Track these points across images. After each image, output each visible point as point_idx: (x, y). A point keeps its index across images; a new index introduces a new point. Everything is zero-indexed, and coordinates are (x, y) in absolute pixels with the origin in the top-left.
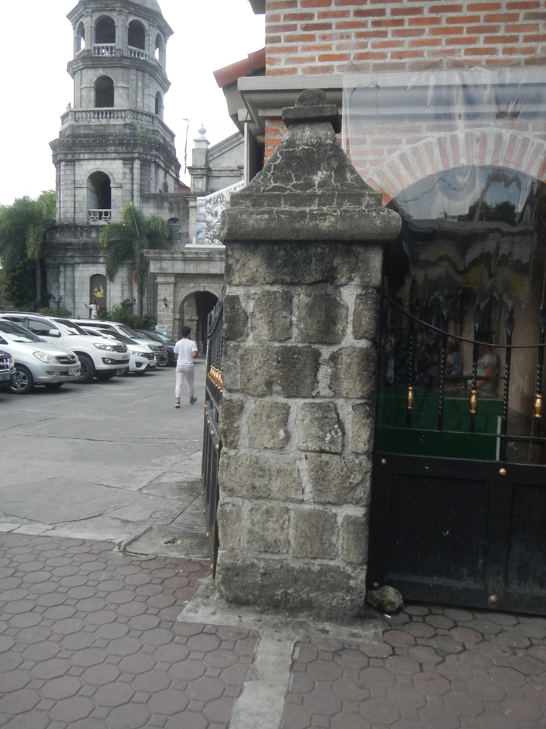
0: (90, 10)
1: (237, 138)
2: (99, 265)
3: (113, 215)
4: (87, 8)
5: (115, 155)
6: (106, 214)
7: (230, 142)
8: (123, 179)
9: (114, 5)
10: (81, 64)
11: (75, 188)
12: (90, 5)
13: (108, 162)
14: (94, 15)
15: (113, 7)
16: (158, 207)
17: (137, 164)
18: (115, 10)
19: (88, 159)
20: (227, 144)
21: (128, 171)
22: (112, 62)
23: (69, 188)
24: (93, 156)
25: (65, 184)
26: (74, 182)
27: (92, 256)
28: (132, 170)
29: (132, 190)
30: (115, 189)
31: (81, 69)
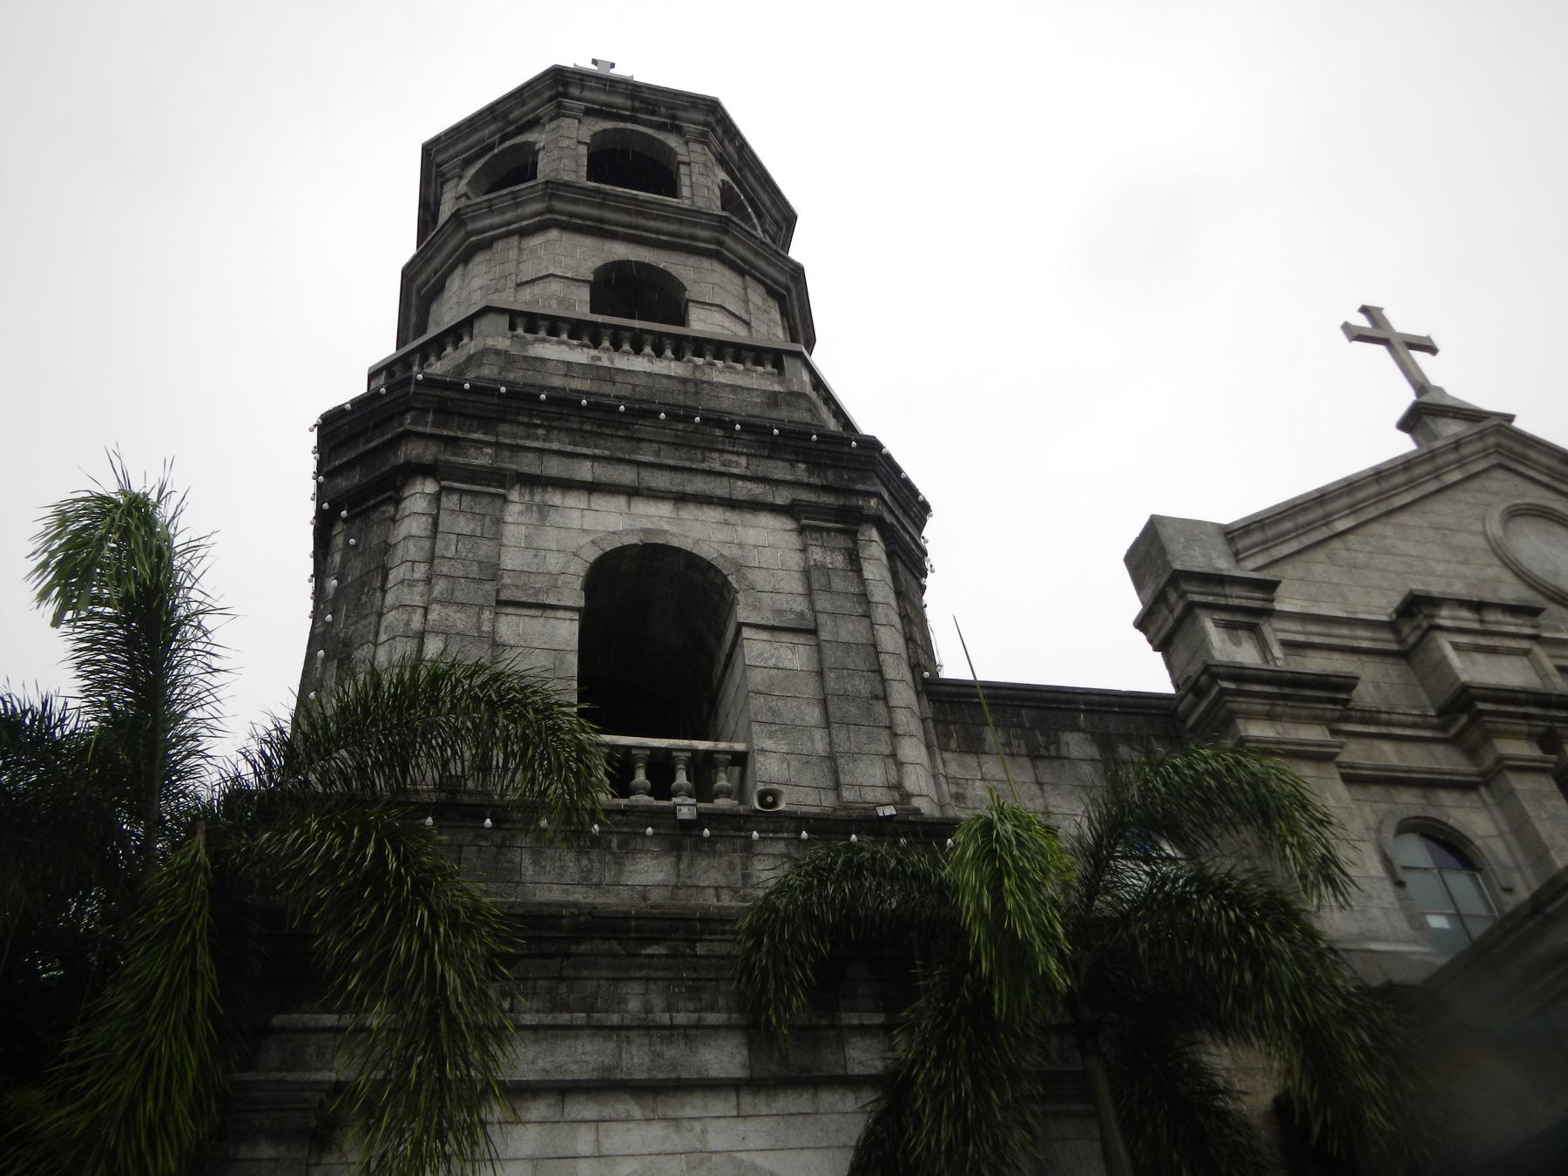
0: (582, 105)
1: (1319, 512)
2: (693, 1107)
3: (770, 768)
4: (565, 95)
5: (758, 490)
6: (702, 766)
7: (1301, 520)
8: (809, 593)
9: (681, 114)
10: (538, 206)
11: (501, 603)
12: (583, 88)
13: (713, 514)
14: (589, 120)
15: (674, 117)
16: (1034, 756)
17: (874, 549)
18: (677, 130)
19: (593, 488)
20: (1288, 525)
21: (839, 560)
22: (687, 230)
23: (459, 596)
24: (627, 476)
25: (428, 581)
26: (492, 571)
27: (648, 1028)
28: (854, 561)
29: (874, 647)
30: (765, 635)
31: (525, 233)
